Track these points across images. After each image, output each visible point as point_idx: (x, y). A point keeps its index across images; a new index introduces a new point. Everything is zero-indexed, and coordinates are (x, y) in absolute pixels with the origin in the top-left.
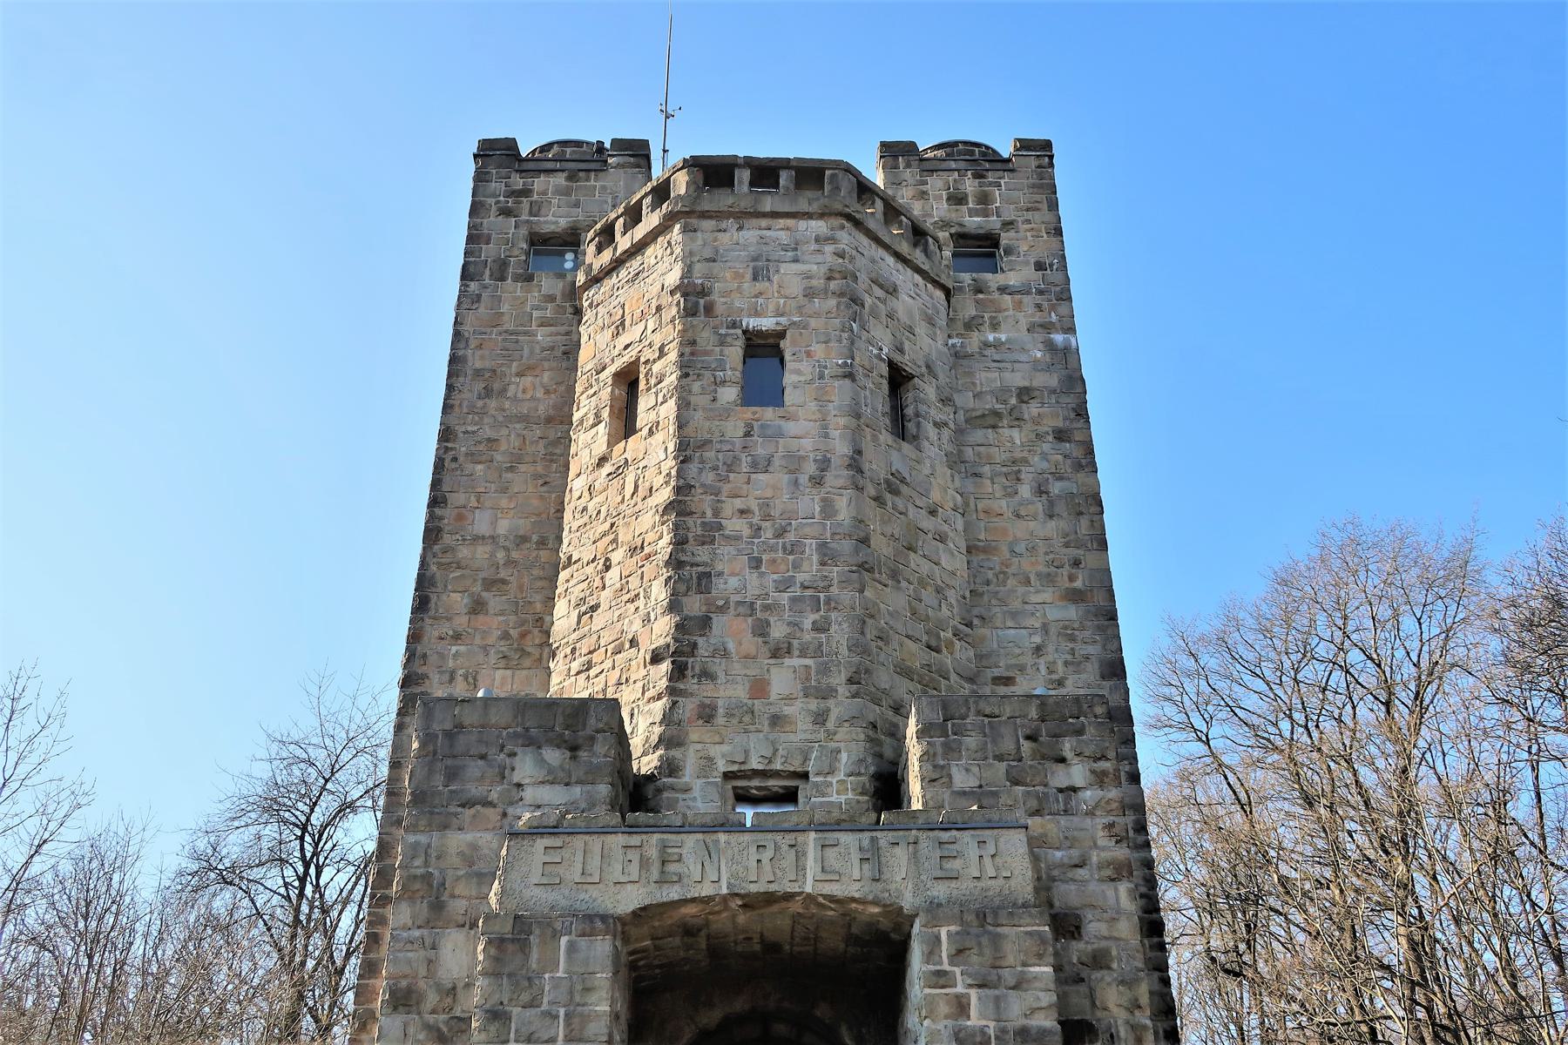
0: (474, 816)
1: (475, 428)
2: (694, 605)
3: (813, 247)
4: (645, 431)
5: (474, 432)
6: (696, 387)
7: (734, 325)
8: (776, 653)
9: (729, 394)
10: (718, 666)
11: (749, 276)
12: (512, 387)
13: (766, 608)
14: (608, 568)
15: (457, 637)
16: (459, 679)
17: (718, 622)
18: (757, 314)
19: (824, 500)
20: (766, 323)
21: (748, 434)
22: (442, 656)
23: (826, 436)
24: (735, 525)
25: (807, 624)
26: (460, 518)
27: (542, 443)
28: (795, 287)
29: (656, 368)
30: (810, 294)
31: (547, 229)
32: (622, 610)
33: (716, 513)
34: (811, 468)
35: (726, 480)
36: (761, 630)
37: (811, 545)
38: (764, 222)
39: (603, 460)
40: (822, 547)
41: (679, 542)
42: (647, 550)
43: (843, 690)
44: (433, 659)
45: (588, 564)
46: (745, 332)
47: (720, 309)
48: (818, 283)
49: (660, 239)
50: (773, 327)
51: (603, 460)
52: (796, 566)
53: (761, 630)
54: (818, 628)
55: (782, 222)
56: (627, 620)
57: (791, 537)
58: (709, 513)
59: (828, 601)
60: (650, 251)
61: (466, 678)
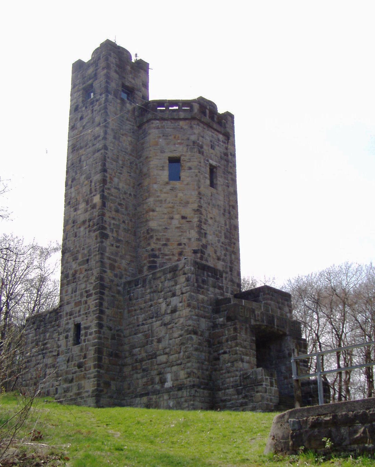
0: (203, 292)
1: (113, 149)
2: (204, 241)
3: (222, 144)
4: (185, 183)
5: (112, 150)
6: (202, 177)
7: (208, 161)
8: (219, 259)
9: (208, 182)
10: (209, 259)
11: (210, 147)
12: (121, 138)
13: (216, 246)
14: (172, 218)
15: (114, 219)
16: (114, 232)
17: (209, 247)
18: (212, 159)
19: (225, 221)
20: (214, 163)
21: (211, 196)
22: (110, 223)
23: (225, 202)
24: (210, 222)
25: (223, 252)
26: (111, 179)
27: (129, 161)
28: (219, 155)
29: (189, 164)
30: (221, 158)
31: (127, 84)
32: (180, 234)
33: (207, 217)
34: (222, 211)
35: (208, 207)
36: (215, 252)
37: (223, 232)
38: (213, 131)
39: (167, 183)
40: (225, 234)
41: (200, 221)
42: (188, 220)
43: (229, 273)
44: (108, 223)
45: (163, 214)
46: (210, 164)
47: (205, 154)
48: (223, 155)
49: (187, 121)
50: (215, 165)
51: (167, 183)
52: (221, 237)
53: (215, 252)
54: (225, 255)
55: (216, 133)
56: (182, 237)
57: (219, 229)
58: (206, 216)
59: (226, 248)
60: (181, 123)
61: (116, 231)
